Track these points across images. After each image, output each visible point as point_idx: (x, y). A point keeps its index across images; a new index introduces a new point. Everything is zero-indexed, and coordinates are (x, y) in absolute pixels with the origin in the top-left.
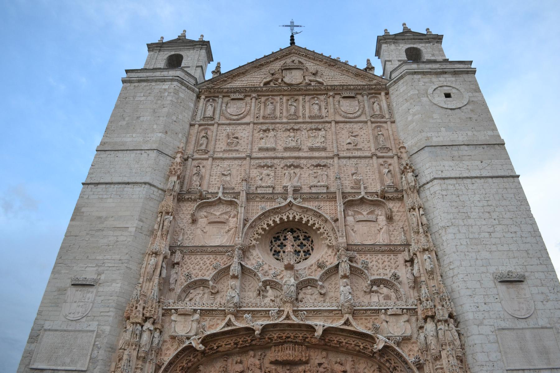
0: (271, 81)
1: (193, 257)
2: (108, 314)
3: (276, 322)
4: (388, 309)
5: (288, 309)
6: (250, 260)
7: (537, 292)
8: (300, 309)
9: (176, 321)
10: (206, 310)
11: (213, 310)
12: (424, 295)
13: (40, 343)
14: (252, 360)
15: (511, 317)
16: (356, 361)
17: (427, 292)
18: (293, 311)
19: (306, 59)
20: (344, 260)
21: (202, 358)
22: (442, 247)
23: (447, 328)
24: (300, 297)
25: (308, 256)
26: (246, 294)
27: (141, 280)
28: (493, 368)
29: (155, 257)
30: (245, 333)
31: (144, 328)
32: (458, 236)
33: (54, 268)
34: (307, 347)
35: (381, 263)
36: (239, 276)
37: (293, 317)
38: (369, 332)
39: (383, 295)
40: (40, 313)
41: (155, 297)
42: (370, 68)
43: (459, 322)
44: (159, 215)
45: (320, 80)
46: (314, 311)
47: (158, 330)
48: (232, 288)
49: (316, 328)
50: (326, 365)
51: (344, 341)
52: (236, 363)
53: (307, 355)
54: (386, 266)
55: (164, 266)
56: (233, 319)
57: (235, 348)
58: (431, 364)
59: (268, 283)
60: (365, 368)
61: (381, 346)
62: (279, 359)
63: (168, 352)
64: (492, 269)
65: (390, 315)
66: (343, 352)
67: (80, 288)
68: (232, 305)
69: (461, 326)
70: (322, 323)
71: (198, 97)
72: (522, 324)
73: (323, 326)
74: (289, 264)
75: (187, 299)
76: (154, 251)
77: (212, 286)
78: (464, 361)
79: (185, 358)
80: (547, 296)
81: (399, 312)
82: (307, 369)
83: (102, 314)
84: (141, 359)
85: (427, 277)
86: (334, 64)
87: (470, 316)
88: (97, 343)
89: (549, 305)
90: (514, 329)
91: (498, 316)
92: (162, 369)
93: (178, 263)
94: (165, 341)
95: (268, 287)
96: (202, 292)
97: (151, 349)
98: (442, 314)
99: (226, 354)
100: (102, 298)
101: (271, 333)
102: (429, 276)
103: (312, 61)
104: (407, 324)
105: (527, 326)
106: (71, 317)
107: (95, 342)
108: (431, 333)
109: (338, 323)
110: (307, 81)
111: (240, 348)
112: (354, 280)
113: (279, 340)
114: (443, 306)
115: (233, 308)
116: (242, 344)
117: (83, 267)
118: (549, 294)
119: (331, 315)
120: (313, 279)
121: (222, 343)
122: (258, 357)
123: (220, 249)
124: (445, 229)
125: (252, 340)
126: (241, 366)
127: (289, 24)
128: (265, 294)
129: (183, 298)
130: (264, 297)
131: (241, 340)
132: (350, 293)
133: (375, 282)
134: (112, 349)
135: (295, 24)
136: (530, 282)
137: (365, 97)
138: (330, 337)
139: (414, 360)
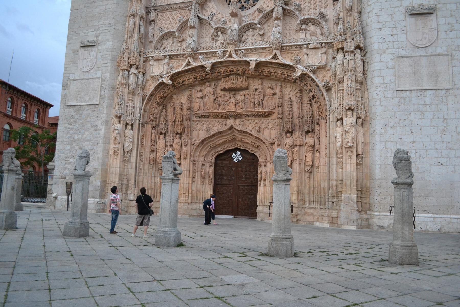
1: (164, 14)
2: (107, 65)
3: (221, 60)
4: (310, 44)
5: (231, 49)
6: (207, 11)
7: (444, 22)
8: (240, 48)
9: (153, 65)
10: (173, 55)
11: (177, 55)
12: (338, 31)
13: (69, 89)
14: (208, 88)
15: (413, 46)
16: (283, 85)
17: (342, 28)
18: (235, 50)
20: (277, 4)
21: (174, 89)
23: (351, 58)
24: (243, 39)
25: (256, 2)
26: (204, 40)
27: (126, 37)
28: (385, 89)
29: (134, 18)
30: (200, 70)
31: (130, 72)
33: (68, 36)
34: (248, 77)
35: (312, 4)
36: (196, 26)
37: (234, 55)
38: (291, 64)
39: (310, 32)
40: (65, 69)
41: (136, 49)
43: (367, 52)
46: (251, 49)
47: (141, 73)
48: (190, 36)
49: (251, 62)
50: (260, 90)
51: (273, 72)
52: (198, 91)
53: (247, 83)
54: (316, 6)
55: (142, 24)
56: (191, 60)
57: (196, 81)
58: (336, 87)
59: (219, 29)
60: (290, 91)
61: (298, 74)
62: (226, 87)
63: (150, 88)
64: (406, 3)
65: (310, 49)
66: (274, 80)
67: (87, 49)
68: (189, 50)
69: (368, 55)
70: (255, 59)
72: (422, 52)
73: (256, 61)
74: (233, 12)
75: (162, 48)
76: (132, 13)
77: (178, 36)
78: (363, 83)
79: (162, 91)
80: (453, 26)
81: (319, 46)
82: (247, 93)
83: (103, 65)
84: (131, 93)
85: (345, 13)
87: (376, 47)
88: (103, 86)
89: (451, 35)
90: (412, 57)
91: (401, 46)
93: (153, 21)
94: (147, 80)
95: (219, 33)
96: (171, 42)
97: (137, 86)
98: (350, 45)
99: (191, 86)
100: (101, 54)
101: (219, 68)
102: (347, 13)
104: (324, 55)
105: (425, 54)
106: (84, 70)
107: (101, 85)
108: (339, 63)
109: (268, 58)
111: (199, 81)
112: (288, 21)
113: (226, 73)
114: (353, 39)
115: (191, 52)
116: (199, 78)
117: (86, 33)
119: (264, 51)
120: (253, 23)
121: (185, 78)
122: (212, 87)
123: (183, 5)
125: (206, 75)
126: (201, 93)
128: (217, 38)
129: (159, 47)
130: (217, 41)
131: (198, 75)
132: (279, 33)
133: (304, 22)
134: (113, 88)
136: (439, 13)
138: (262, 69)
139: (323, 83)
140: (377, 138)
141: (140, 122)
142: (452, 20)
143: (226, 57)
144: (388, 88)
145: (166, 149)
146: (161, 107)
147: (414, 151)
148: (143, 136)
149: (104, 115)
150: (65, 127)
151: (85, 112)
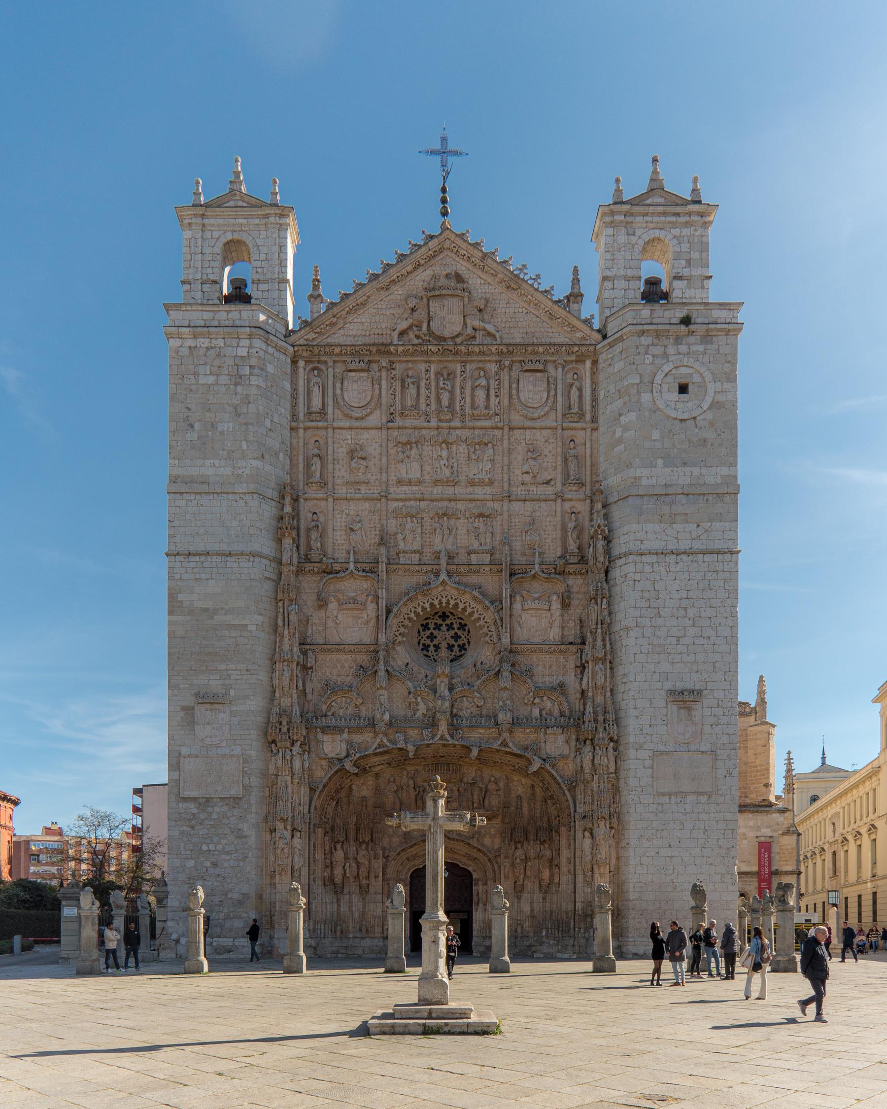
0: (410, 327)
19: (470, 266)
22: (619, 653)
31: (294, 752)
32: (641, 641)
42: (575, 296)
44: (280, 604)
45: (490, 328)
61: (535, 769)
71: (294, 362)
86: (515, 287)
87: (632, 739)
92: (317, 793)
103: (480, 273)
110: (469, 331)
118: (721, 717)
123: (359, 647)
124: (628, 631)
127: (438, 146)
135: (451, 147)
136: (705, 702)
137: (560, 370)
140: (631, 853)
141: (311, 826)
142: (719, 712)
143: (436, 739)
144: (644, 792)
145: (348, 864)
146: (335, 803)
147: (671, 867)
148: (314, 846)
149: (253, 815)
150: (182, 833)
151: (217, 809)
